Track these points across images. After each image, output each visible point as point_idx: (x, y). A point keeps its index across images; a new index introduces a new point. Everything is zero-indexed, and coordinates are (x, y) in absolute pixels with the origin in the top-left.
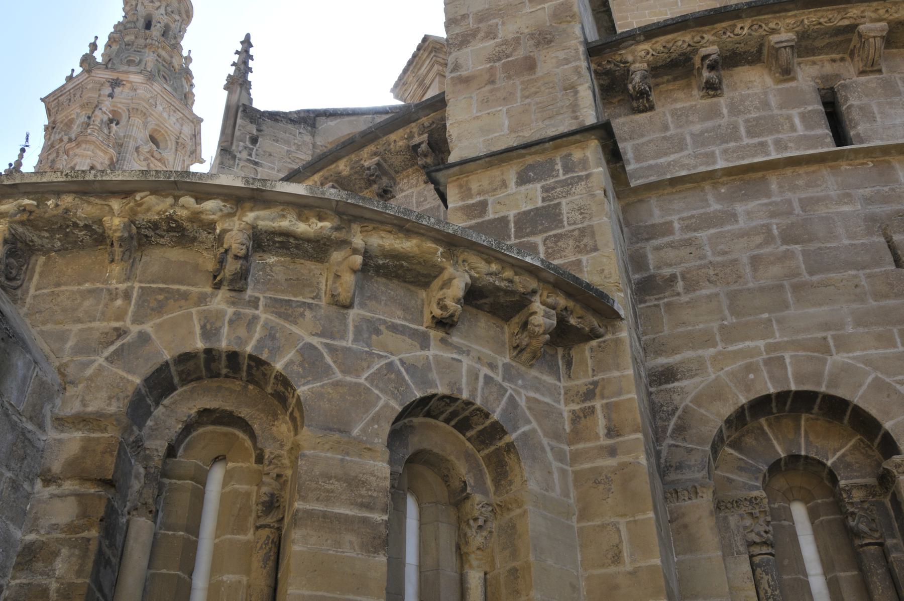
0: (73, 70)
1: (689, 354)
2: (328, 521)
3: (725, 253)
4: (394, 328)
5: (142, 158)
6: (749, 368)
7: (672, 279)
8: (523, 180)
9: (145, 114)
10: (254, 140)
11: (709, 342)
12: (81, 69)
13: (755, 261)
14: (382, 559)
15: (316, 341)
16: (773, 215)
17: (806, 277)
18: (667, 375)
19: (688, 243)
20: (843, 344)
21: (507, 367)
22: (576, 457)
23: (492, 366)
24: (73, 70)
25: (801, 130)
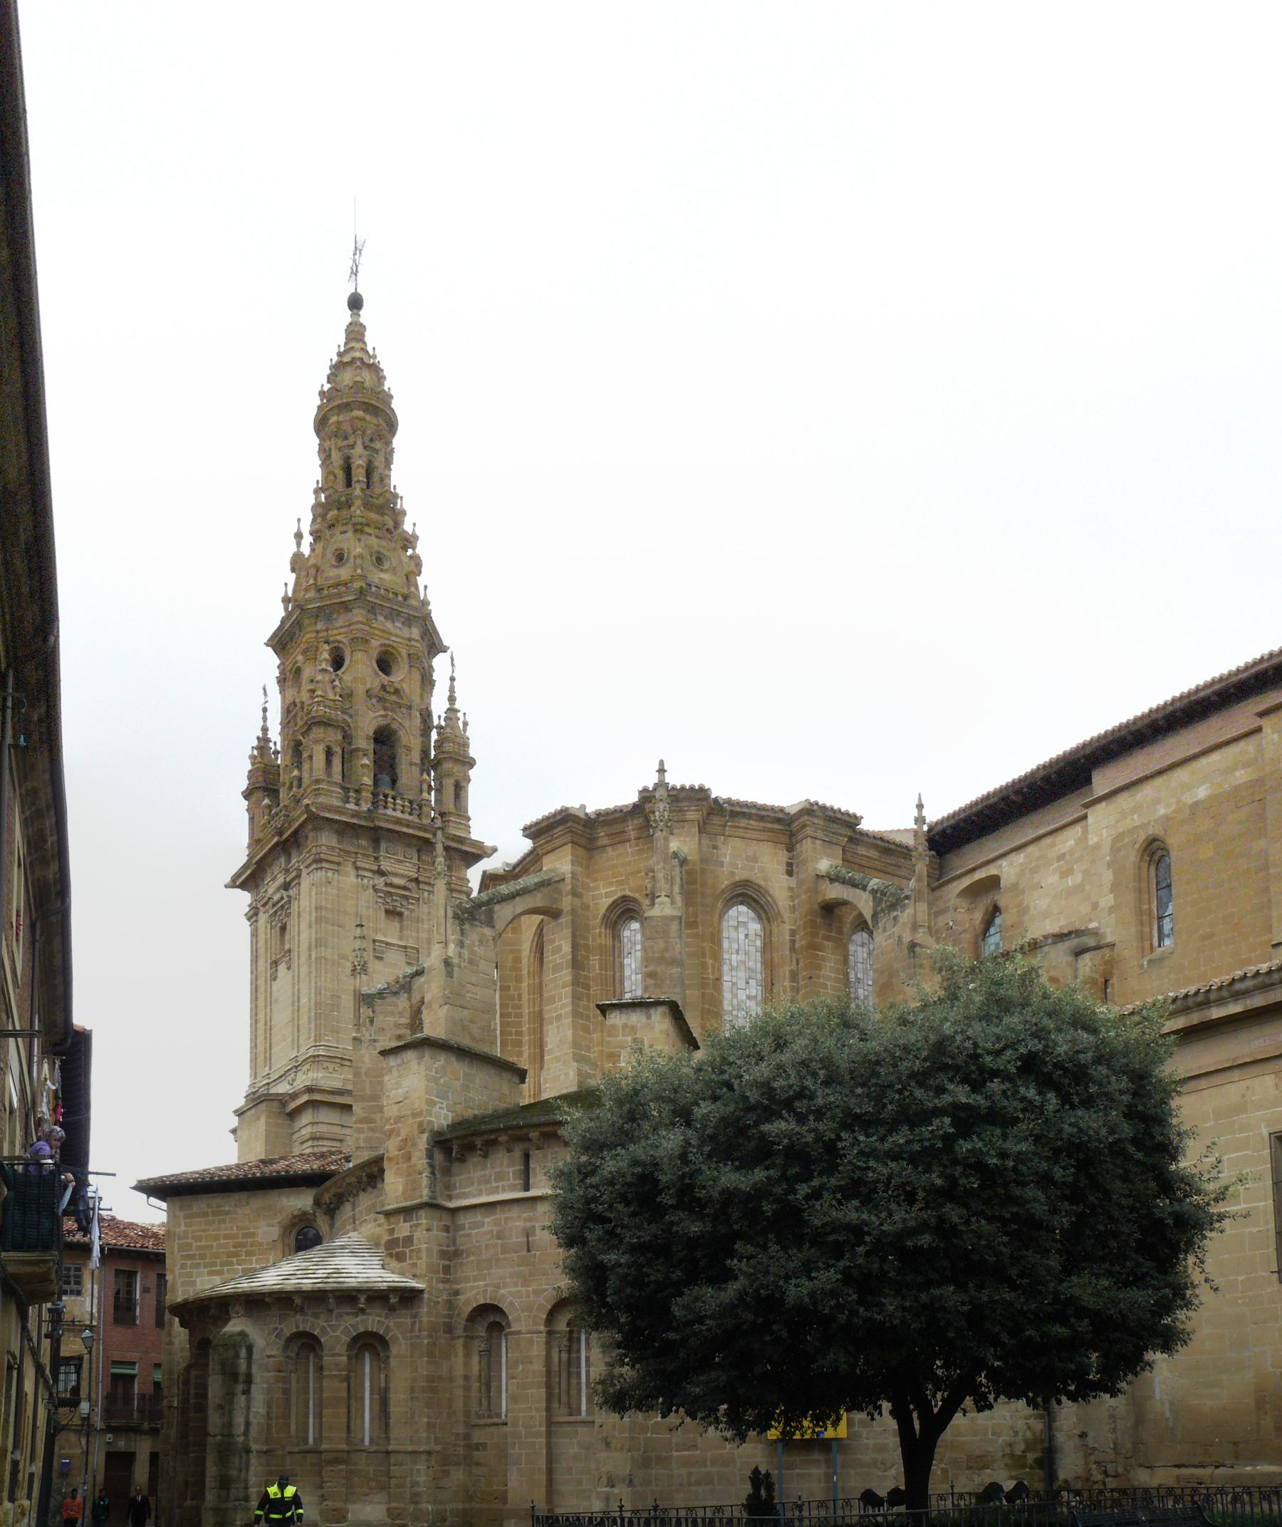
0: (286, 584)
1: (463, 1285)
2: (332, 1377)
3: (477, 1242)
4: (347, 1314)
5: (374, 701)
6: (478, 1293)
7: (462, 1252)
8: (405, 1221)
9: (367, 641)
10: (372, 1021)
11: (469, 1281)
12: (294, 576)
13: (487, 1246)
14: (345, 1384)
15: (325, 1324)
16: (496, 1225)
17: (500, 1256)
18: (457, 1293)
19: (469, 1235)
20: (505, 1285)
21: (386, 1315)
22: (411, 1338)
23: (380, 1316)
24: (286, 584)
25: (511, 1181)
